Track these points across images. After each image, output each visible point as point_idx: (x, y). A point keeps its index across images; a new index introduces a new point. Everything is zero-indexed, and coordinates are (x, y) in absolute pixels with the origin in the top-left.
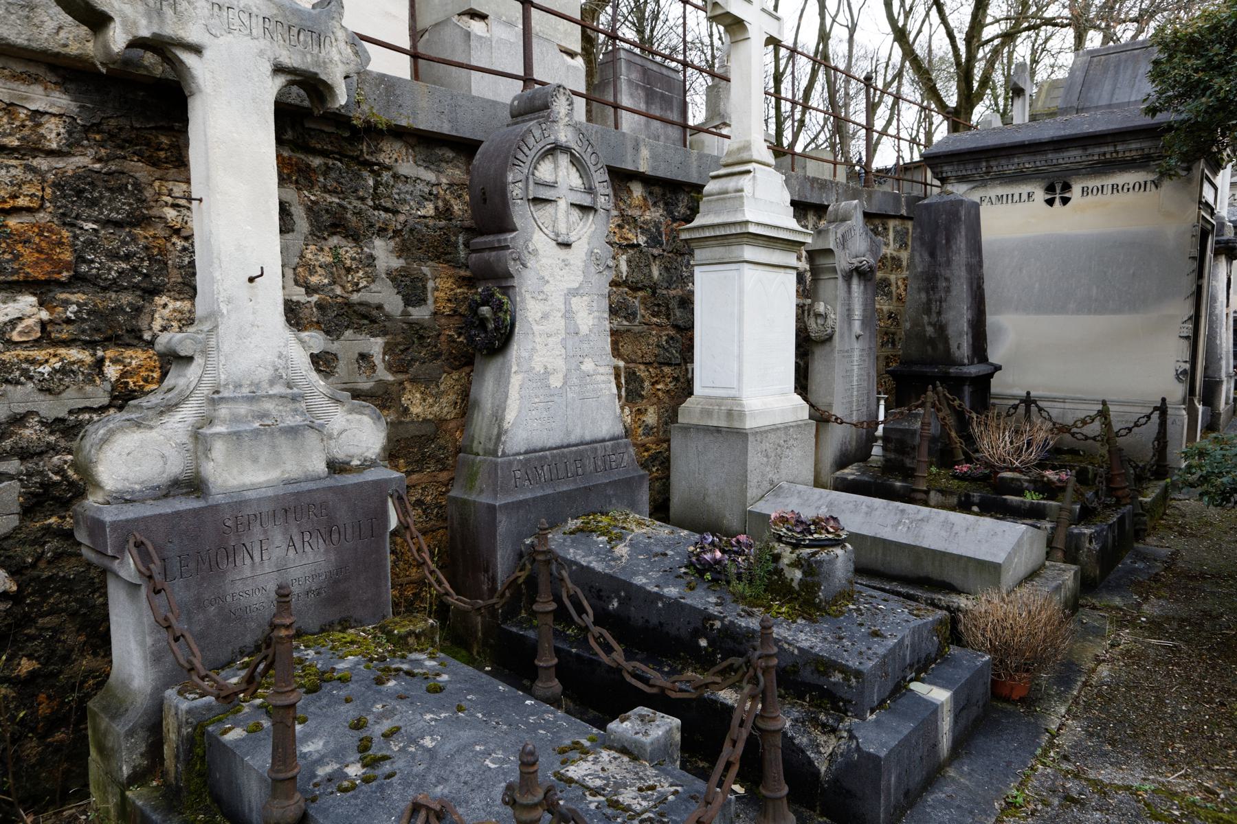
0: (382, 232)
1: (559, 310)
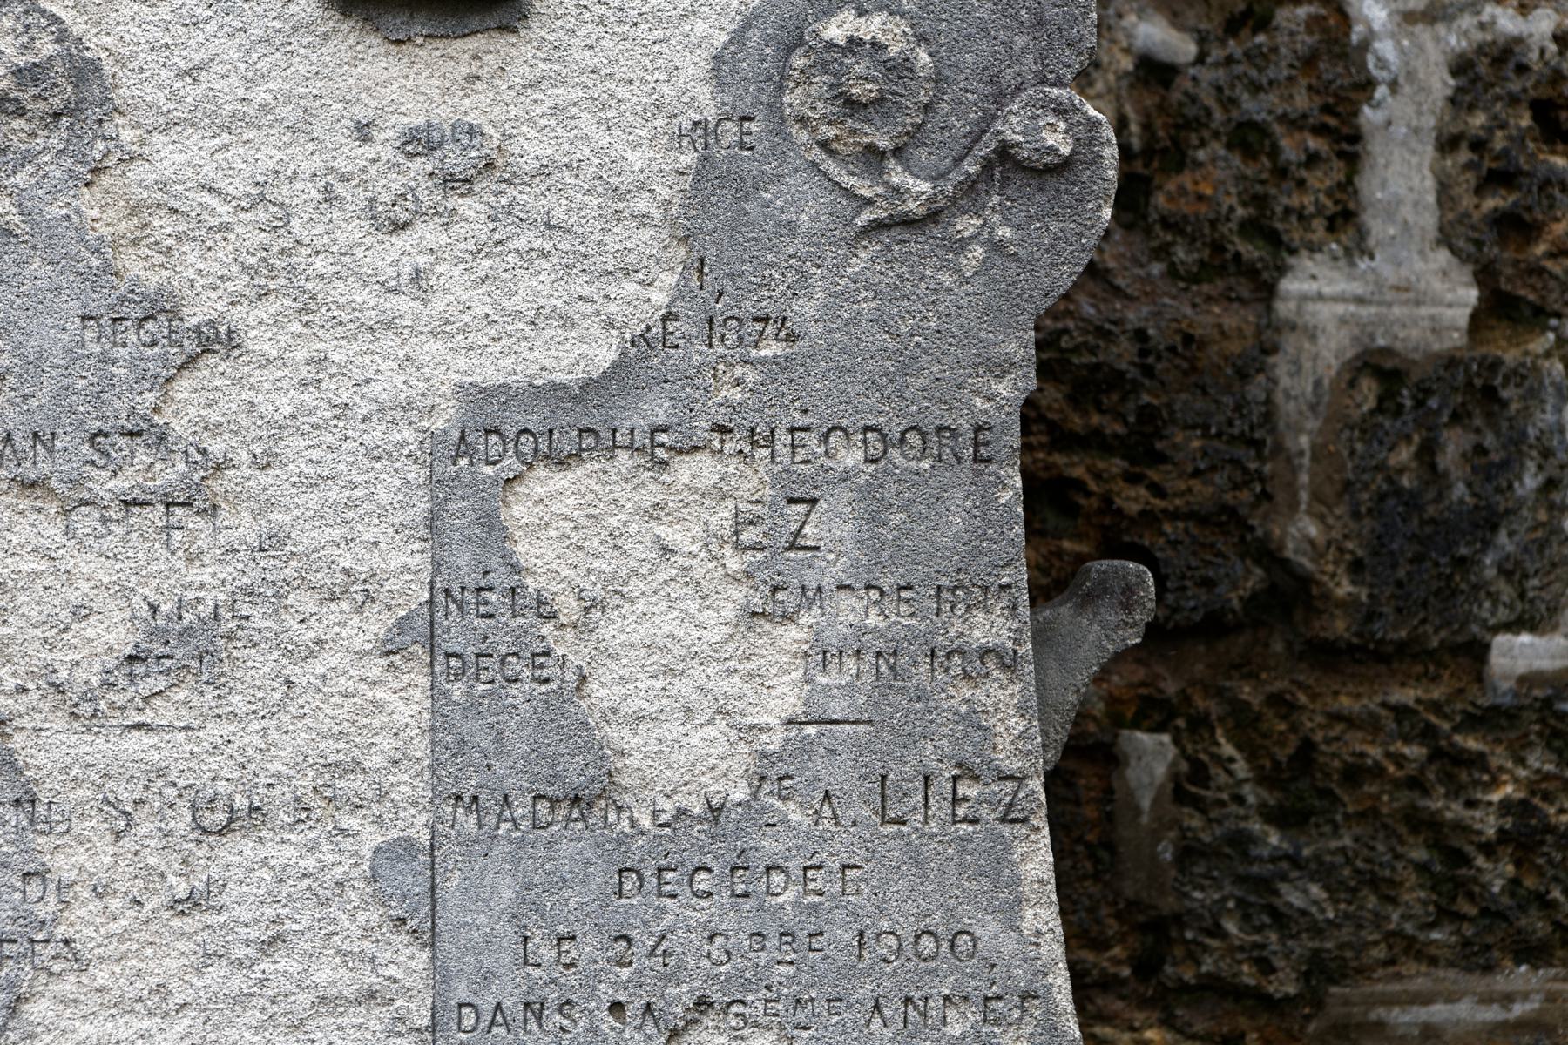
1: (362, 591)
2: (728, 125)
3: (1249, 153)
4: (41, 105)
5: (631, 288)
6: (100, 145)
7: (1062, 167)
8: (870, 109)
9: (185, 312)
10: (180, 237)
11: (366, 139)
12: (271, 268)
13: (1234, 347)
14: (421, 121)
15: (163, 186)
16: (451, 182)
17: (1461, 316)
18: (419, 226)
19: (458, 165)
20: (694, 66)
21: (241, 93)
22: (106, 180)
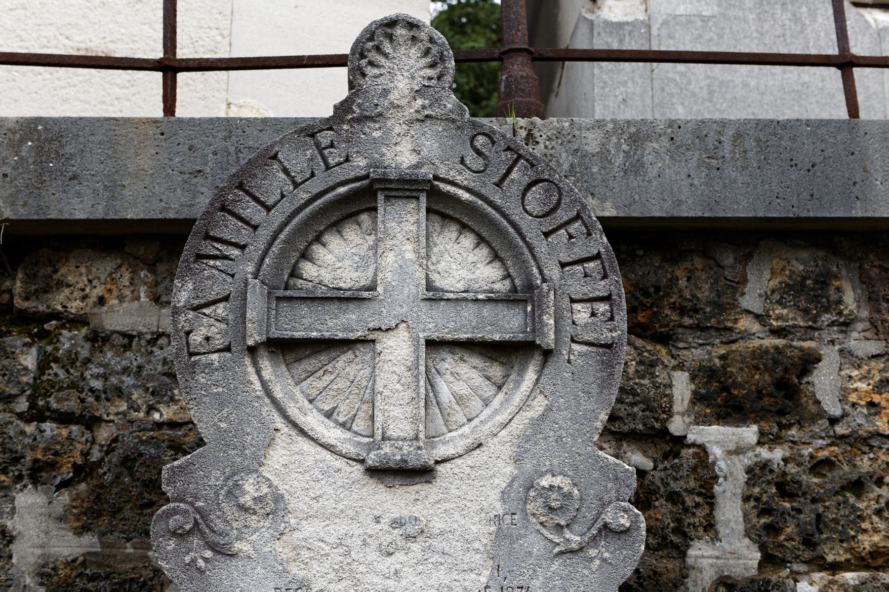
0: (37, 474)
2: (507, 516)
3: (674, 503)
4: (262, 511)
5: (473, 576)
6: (283, 525)
7: (627, 531)
8: (557, 510)
9: (312, 586)
10: (310, 558)
11: (378, 522)
12: (344, 569)
13: (672, 576)
14: (398, 516)
15: (305, 540)
16: (409, 538)
17: (755, 563)
18: (397, 554)
19: (411, 531)
20: (495, 495)
21: (334, 506)
22: (284, 538)
